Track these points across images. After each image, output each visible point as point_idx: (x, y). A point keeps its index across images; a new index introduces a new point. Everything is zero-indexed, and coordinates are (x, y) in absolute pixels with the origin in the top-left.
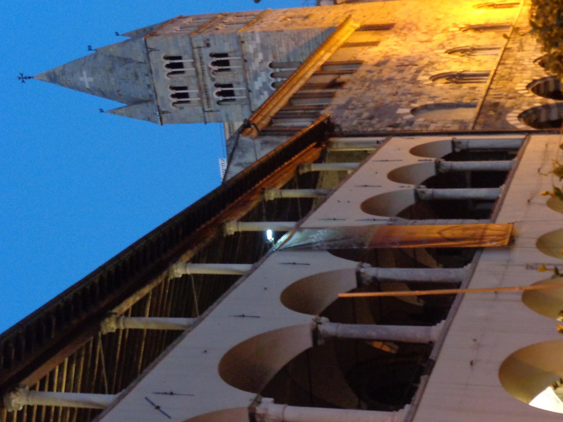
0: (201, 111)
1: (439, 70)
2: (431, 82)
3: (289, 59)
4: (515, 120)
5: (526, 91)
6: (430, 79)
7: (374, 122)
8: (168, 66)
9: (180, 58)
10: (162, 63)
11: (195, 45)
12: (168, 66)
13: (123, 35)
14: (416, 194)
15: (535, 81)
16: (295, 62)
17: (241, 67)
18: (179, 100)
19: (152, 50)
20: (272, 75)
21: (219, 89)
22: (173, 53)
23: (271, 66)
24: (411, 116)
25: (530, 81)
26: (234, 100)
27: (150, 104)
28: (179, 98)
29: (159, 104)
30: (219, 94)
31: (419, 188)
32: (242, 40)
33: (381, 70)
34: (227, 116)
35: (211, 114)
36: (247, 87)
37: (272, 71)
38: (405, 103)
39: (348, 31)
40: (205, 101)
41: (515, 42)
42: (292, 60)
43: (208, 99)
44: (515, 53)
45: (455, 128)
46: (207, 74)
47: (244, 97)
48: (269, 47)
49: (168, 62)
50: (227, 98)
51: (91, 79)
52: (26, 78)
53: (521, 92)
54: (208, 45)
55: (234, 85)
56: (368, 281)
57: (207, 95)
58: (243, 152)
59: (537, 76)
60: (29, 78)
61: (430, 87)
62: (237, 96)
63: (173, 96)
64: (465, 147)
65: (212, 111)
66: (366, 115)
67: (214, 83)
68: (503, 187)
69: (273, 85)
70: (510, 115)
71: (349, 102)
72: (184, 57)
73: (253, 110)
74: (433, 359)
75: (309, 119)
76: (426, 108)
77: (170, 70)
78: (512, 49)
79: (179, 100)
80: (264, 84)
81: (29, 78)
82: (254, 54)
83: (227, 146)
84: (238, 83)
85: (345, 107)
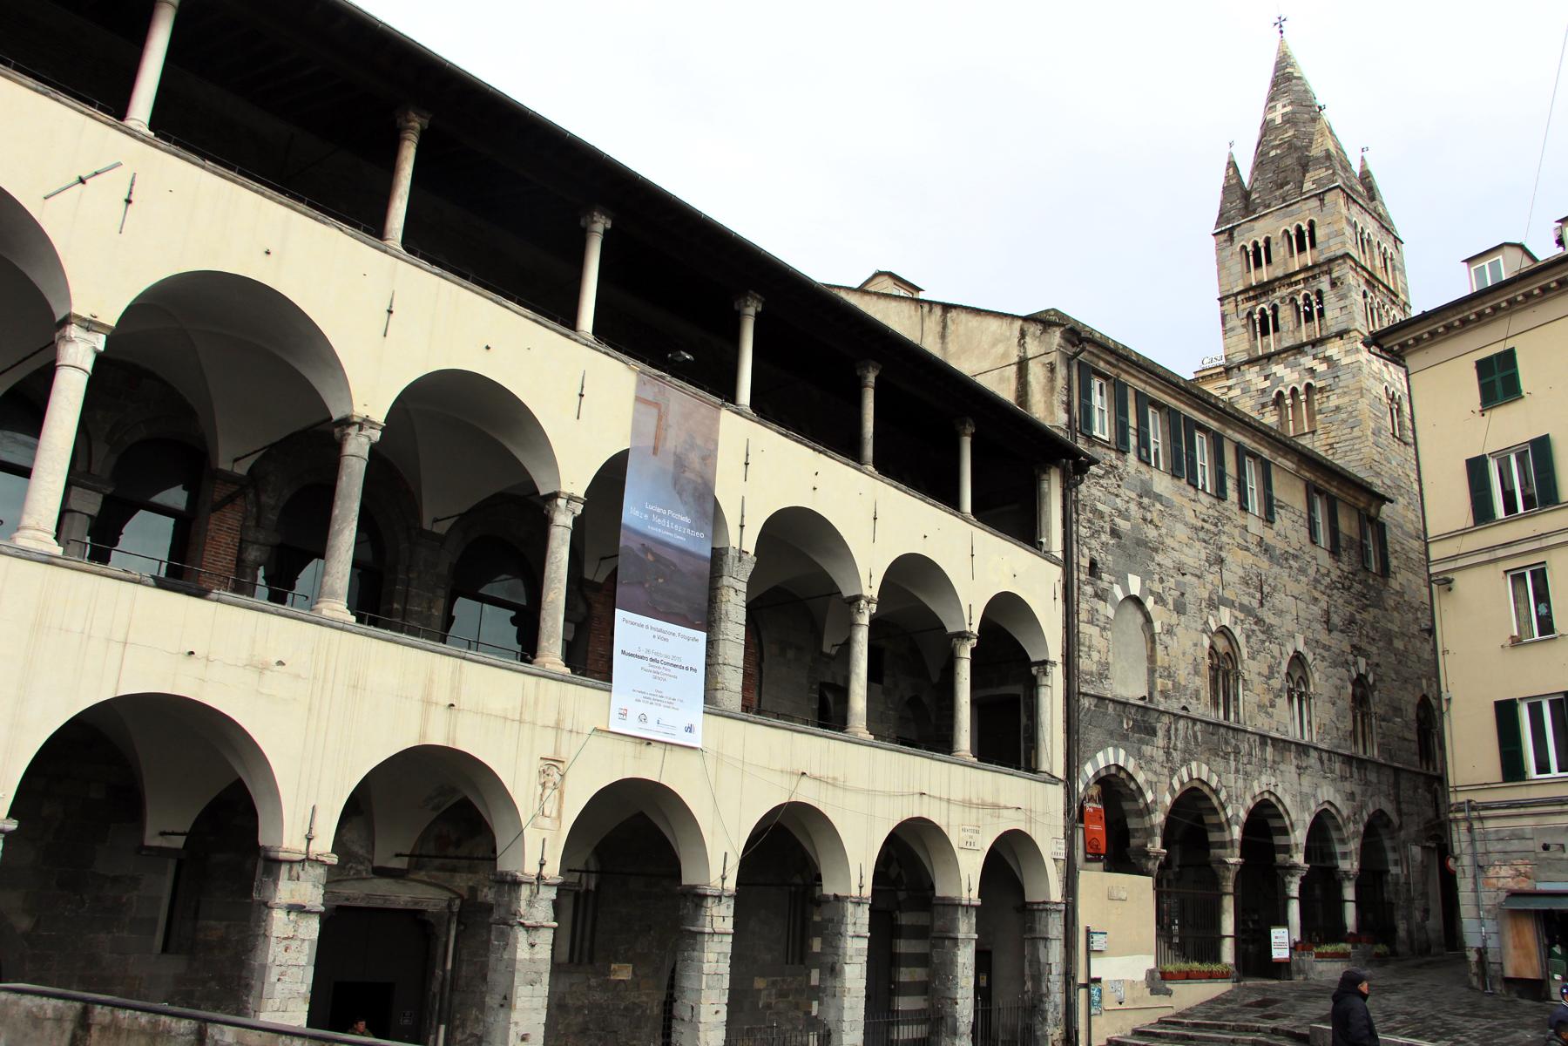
0: (1235, 290)
1: (1248, 642)
2: (1214, 628)
3: (1320, 412)
4: (1107, 760)
5: (1186, 779)
6: (1225, 626)
7: (1104, 537)
8: (1299, 228)
9: (1313, 245)
10: (1303, 220)
11: (1332, 265)
12: (1299, 228)
13: (1363, 159)
14: (858, 598)
15: (1216, 792)
16: (1316, 421)
17: (1305, 340)
18: (1251, 254)
19: (1322, 200)
20: (1294, 390)
21: (1269, 312)
22: (1319, 233)
23: (1309, 386)
24: (1120, 595)
25: (1214, 784)
26: (1256, 338)
27: (1243, 212)
28: (1253, 253)
29: (1242, 226)
30: (1263, 311)
31: (869, 603)
32: (1345, 336)
33: (1247, 549)
34: (1232, 329)
35: (1233, 304)
36: (1273, 354)
37: (1301, 389)
38: (1157, 587)
39: (1356, 499)
40: (1251, 294)
41: (1326, 762)
42: (1318, 417)
43: (1254, 298)
44: (1294, 760)
45: (1086, 664)
46: (1290, 290)
47: (1260, 353)
48: (1337, 380)
49: (1305, 228)
50: (1258, 326)
51: (1279, 121)
52: (1281, 26)
53: (1184, 770)
54: (1333, 284)
55: (1277, 334)
56: (549, 512)
57: (1260, 294)
58: (1039, 337)
59: (1229, 796)
60: (1281, 32)
61: (1200, 627)
62: (1262, 340)
63: (1255, 244)
64: (1039, 682)
65: (1237, 306)
66: (1123, 525)
67: (1277, 302)
68: (865, 735)
69: (1280, 394)
70: (1122, 752)
71: (1158, 498)
72: (1315, 252)
73: (1242, 368)
74: (212, 596)
75: (1114, 437)
76: (1148, 620)
77: (1293, 232)
78: (1304, 757)
79: (1251, 254)
80: (1282, 378)
81: (1281, 32)
82: (1325, 357)
83: (1047, 311)
84: (1280, 340)
85: (1146, 491)
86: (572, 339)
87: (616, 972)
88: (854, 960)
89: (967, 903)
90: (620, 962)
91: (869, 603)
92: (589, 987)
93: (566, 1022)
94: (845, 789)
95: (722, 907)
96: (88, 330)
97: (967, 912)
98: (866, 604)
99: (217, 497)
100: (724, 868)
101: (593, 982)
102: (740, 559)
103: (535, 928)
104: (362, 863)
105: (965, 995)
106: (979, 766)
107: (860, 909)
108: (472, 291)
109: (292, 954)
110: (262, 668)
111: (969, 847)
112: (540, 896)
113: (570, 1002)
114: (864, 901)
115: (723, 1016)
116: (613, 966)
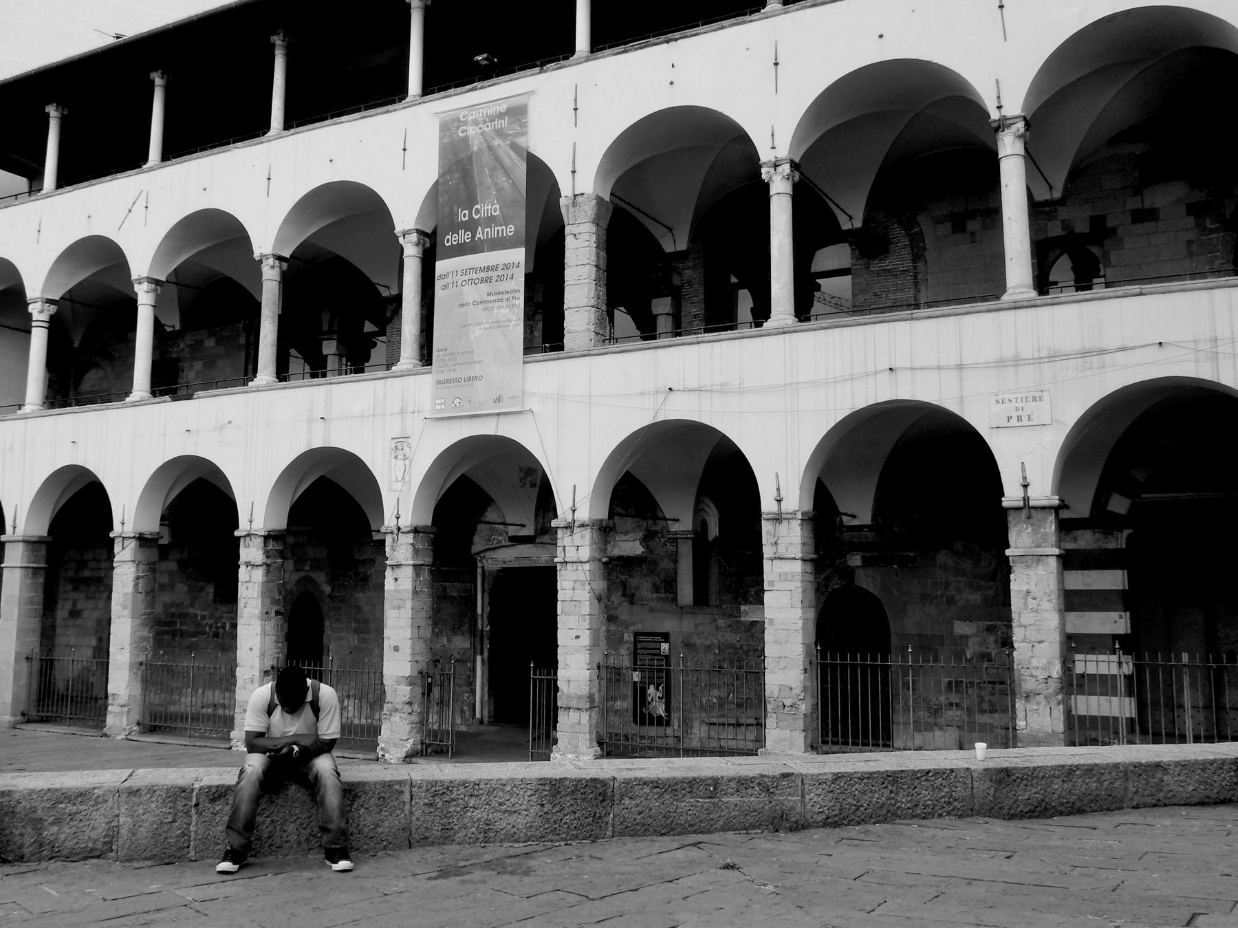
74: (195, 396)
86: (392, 111)
87: (747, 613)
88: (777, 586)
89: (1021, 504)
90: (750, 603)
91: (776, 166)
92: (717, 627)
93: (696, 659)
94: (742, 392)
95: (574, 537)
96: (140, 283)
97: (1029, 517)
98: (772, 170)
99: (388, 314)
100: (574, 501)
101: (721, 623)
102: (574, 205)
103: (398, 566)
104: (501, 535)
105: (1032, 634)
106: (1039, 302)
107: (783, 528)
108: (317, 128)
109: (250, 591)
110: (221, 428)
111: (1017, 423)
112: (399, 542)
113: (699, 642)
114: (784, 516)
115: (586, 639)
116: (743, 608)
